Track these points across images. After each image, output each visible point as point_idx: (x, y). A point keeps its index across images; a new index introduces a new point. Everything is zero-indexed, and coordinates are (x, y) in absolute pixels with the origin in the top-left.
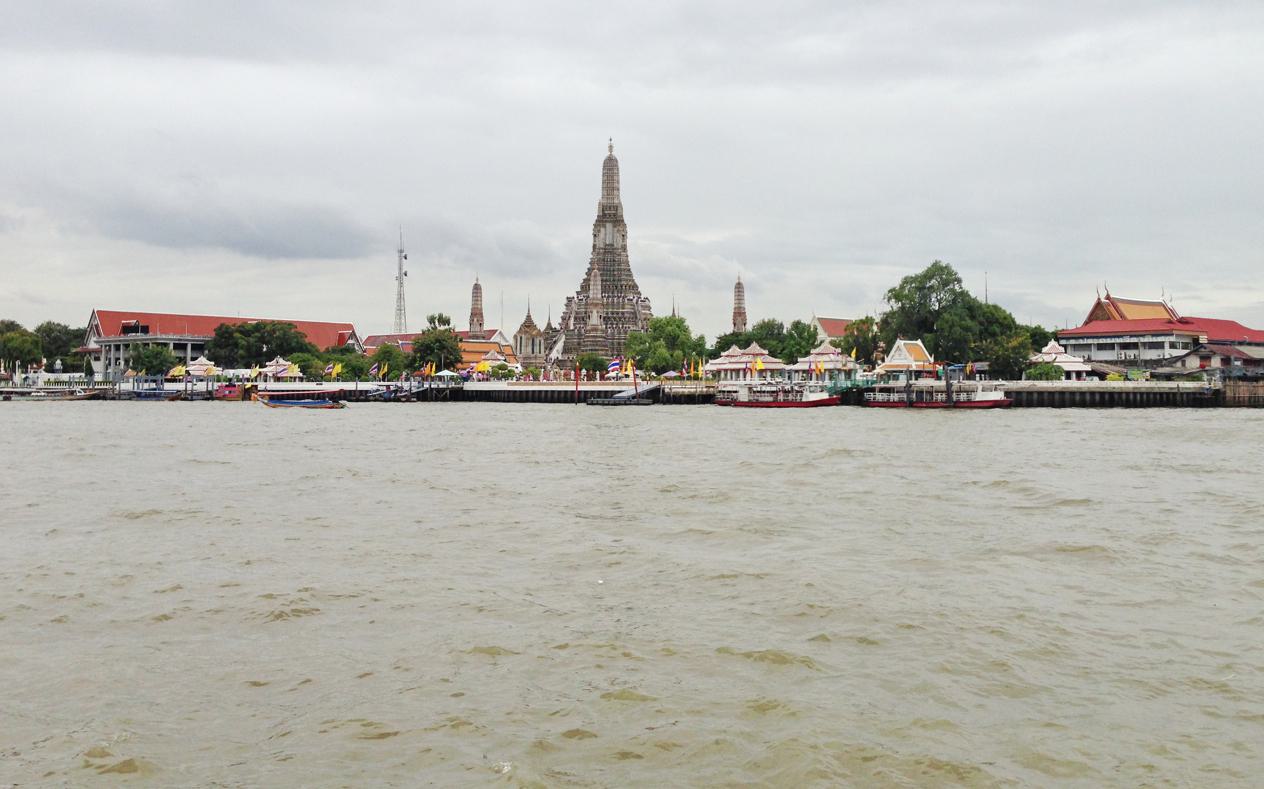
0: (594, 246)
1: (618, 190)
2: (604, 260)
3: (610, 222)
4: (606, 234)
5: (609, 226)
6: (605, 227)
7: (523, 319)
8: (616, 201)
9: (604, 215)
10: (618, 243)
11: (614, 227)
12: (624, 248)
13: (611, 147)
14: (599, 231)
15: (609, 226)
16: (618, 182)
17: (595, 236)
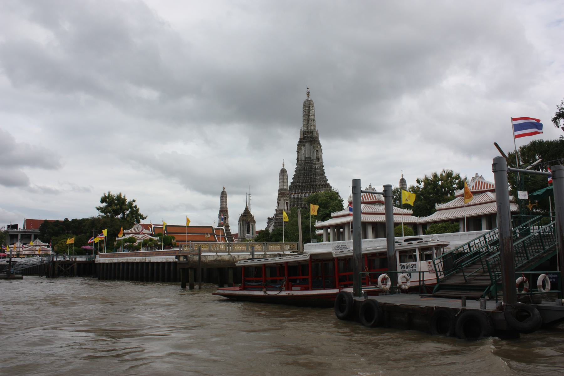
0: (298, 159)
1: (314, 120)
2: (304, 168)
3: (308, 142)
4: (305, 151)
5: (307, 145)
6: (304, 146)
7: (242, 211)
8: (312, 128)
9: (304, 138)
10: (314, 156)
11: (311, 145)
12: (319, 159)
13: (308, 94)
14: (301, 149)
15: (307, 145)
16: (314, 115)
17: (298, 152)
